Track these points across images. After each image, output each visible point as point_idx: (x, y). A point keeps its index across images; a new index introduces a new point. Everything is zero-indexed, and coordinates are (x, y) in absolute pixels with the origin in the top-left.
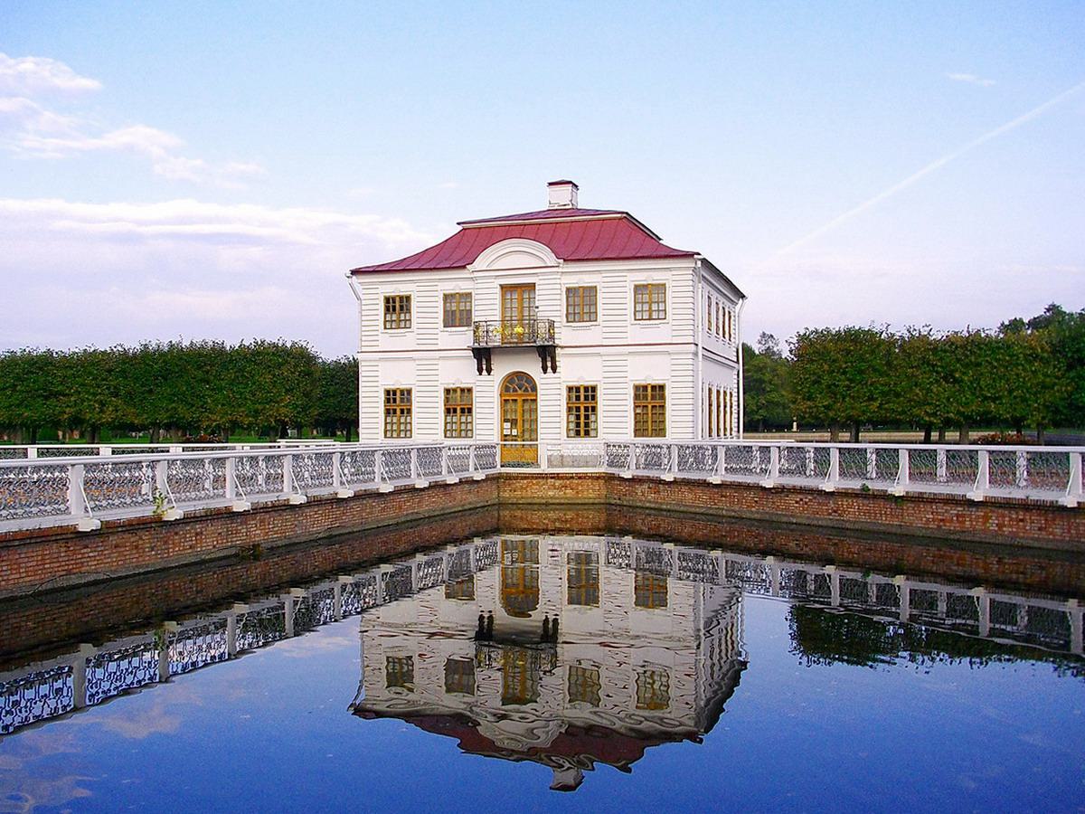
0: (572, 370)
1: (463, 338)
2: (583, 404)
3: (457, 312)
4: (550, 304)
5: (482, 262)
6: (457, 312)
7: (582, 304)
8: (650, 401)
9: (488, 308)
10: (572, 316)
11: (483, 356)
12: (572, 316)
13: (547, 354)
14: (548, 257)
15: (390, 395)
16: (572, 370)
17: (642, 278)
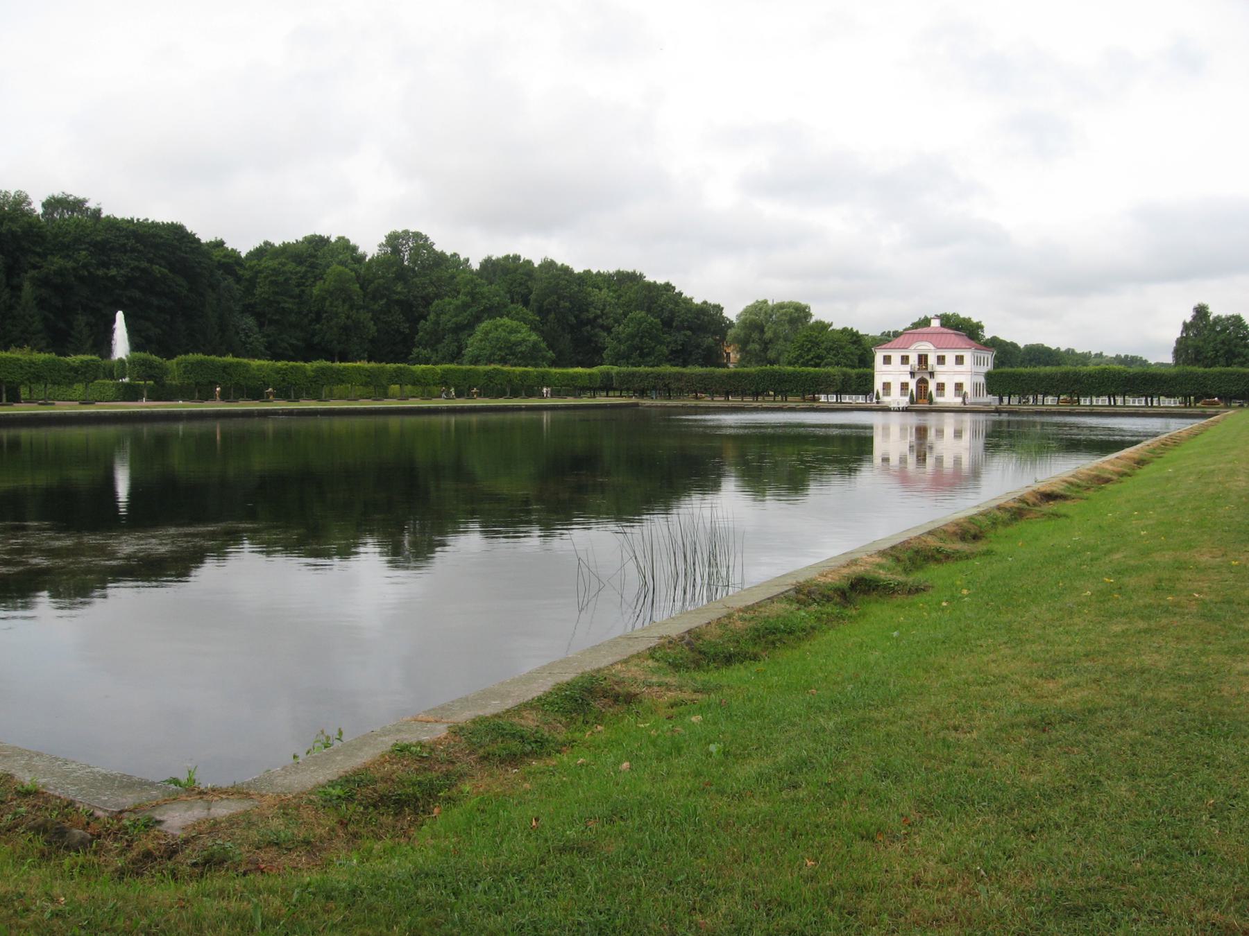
0: (939, 378)
1: (908, 368)
2: (941, 387)
3: (905, 360)
4: (932, 360)
5: (912, 347)
6: (905, 360)
7: (941, 360)
8: (959, 386)
9: (914, 360)
10: (938, 363)
11: (912, 374)
12: (938, 363)
13: (932, 374)
14: (932, 347)
15: (884, 384)
16: (939, 378)
17: (958, 354)
